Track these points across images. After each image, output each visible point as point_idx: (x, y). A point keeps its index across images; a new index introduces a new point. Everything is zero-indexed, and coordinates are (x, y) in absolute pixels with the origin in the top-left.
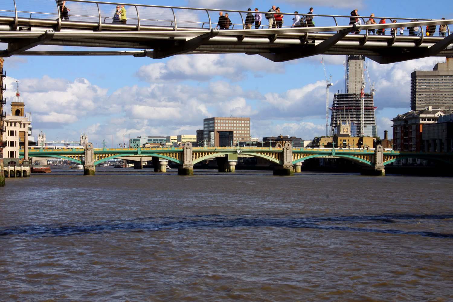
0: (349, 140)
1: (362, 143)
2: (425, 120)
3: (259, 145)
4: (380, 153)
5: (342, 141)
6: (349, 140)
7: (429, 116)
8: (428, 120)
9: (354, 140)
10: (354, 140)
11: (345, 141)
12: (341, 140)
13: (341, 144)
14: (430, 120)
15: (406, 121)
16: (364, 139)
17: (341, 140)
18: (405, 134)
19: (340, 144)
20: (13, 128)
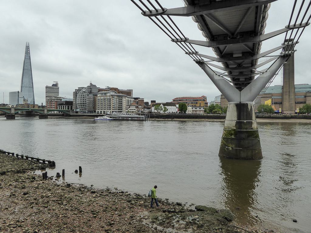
11: (28, 105)
15: (51, 100)
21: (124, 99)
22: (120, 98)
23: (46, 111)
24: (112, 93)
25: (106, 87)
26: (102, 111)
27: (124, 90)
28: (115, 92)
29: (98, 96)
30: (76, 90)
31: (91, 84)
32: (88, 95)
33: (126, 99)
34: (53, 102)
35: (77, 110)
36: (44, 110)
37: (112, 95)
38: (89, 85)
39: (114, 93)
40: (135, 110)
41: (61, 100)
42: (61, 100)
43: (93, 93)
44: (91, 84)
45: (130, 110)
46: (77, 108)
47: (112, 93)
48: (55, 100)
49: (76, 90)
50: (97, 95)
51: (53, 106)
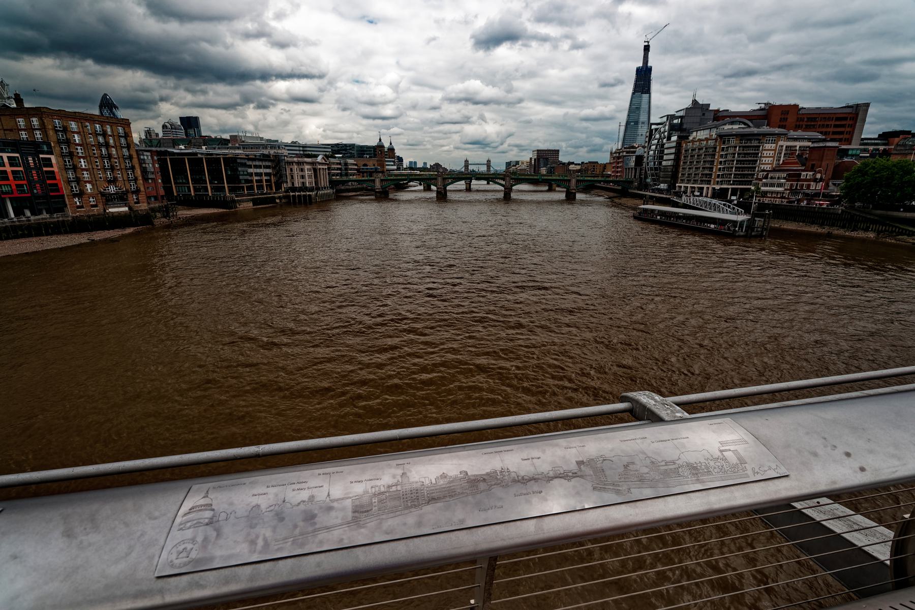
20: (302, 167)
21: (768, 146)
22: (755, 143)
23: (573, 181)
24: (730, 127)
25: (757, 107)
26: (689, 185)
28: (745, 124)
29: (691, 138)
31: (695, 102)
32: (669, 138)
35: (648, 180)
36: (569, 181)
38: (688, 103)
40: (780, 185)
41: (634, 152)
42: (634, 152)
44: (695, 102)
45: (766, 185)
47: (727, 127)
50: (687, 137)
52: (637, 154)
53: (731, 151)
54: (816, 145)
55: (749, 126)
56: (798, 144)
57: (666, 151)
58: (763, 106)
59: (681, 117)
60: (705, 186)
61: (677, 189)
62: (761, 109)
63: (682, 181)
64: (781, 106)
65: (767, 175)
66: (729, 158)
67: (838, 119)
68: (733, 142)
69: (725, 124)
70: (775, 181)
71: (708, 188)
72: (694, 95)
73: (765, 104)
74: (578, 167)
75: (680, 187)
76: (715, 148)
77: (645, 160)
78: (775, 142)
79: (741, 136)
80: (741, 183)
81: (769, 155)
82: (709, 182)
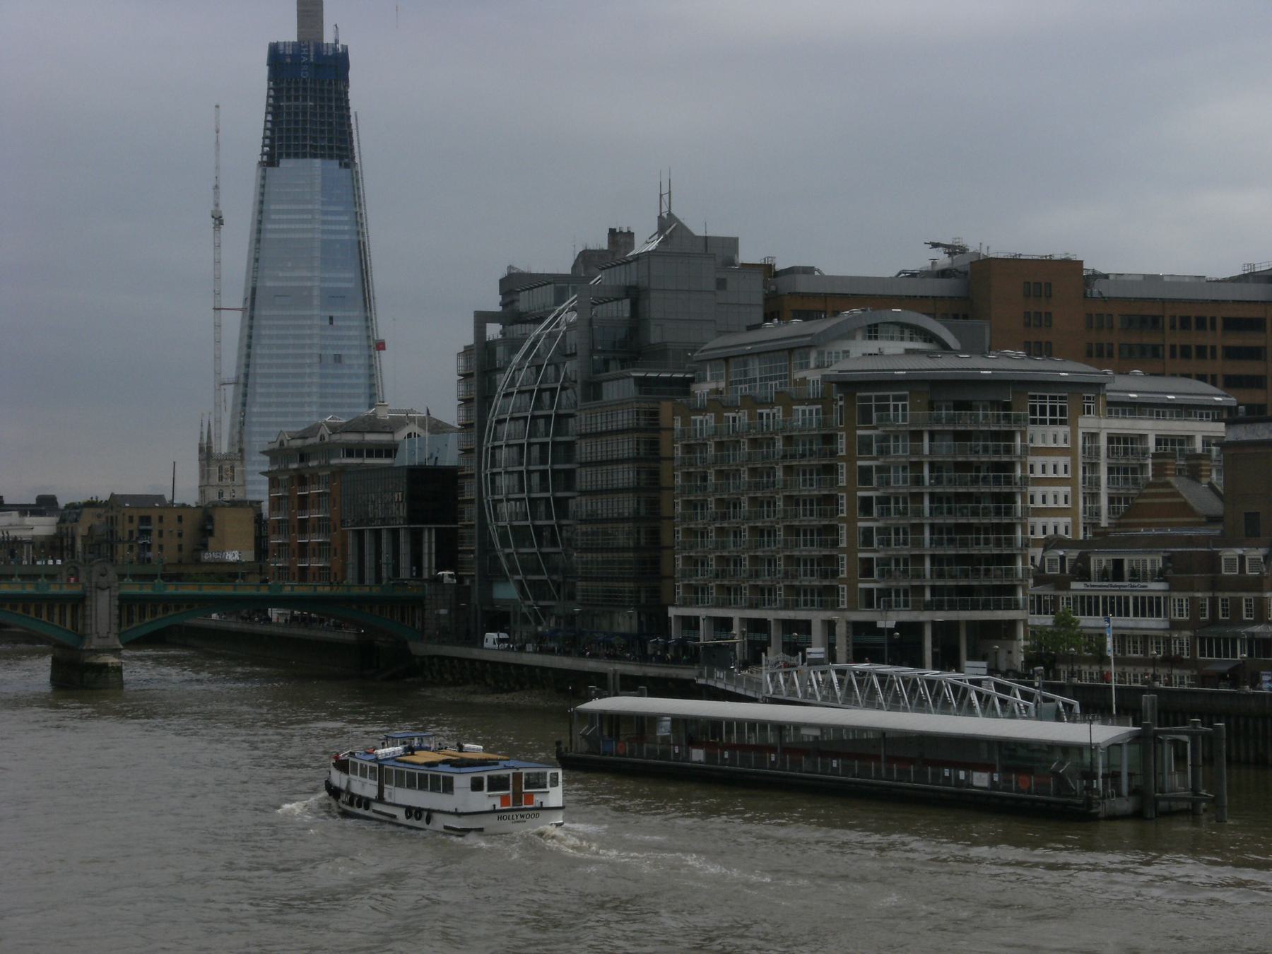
0: (161, 519)
1: (209, 527)
2: (360, 455)
3: (24, 510)
4: (107, 593)
5: (136, 520)
6: (161, 519)
7: (370, 437)
8: (370, 455)
9: (180, 519)
10: (180, 519)
11: (146, 520)
12: (131, 519)
13: (131, 532)
14: (379, 455)
15: (303, 456)
16: (218, 515)
17: (131, 519)
18: (303, 503)
19: (127, 533)
22: (984, 420)
24: (872, 346)
25: (922, 259)
26: (735, 614)
27: (1177, 282)
28: (929, 337)
29: (702, 389)
30: (482, 319)
31: (669, 225)
32: (592, 390)
33: (1087, 423)
34: (316, 479)
35: (506, 592)
36: (78, 603)
37: (849, 386)
39: (894, 347)
42: (390, 450)
43: (659, 354)
44: (669, 225)
45: (1089, 606)
46: (492, 573)
48: (327, 450)
49: (482, 319)
51: (322, 526)
52: (404, 459)
53: (901, 452)
54: (1243, 433)
55: (945, 347)
56: (1150, 428)
57: (584, 450)
58: (943, 259)
59: (635, 295)
60: (817, 617)
61: (676, 632)
62: (943, 274)
63: (696, 594)
64: (1015, 264)
65: (1084, 559)
66: (900, 484)
67: (1233, 324)
68: (903, 415)
69: (850, 336)
70: (1125, 589)
71: (830, 626)
72: (665, 196)
73: (952, 250)
74: (43, 526)
75: (690, 623)
76: (829, 439)
77: (470, 491)
78: (1059, 416)
79: (934, 390)
80: (965, 596)
81: (1055, 483)
82: (827, 597)
